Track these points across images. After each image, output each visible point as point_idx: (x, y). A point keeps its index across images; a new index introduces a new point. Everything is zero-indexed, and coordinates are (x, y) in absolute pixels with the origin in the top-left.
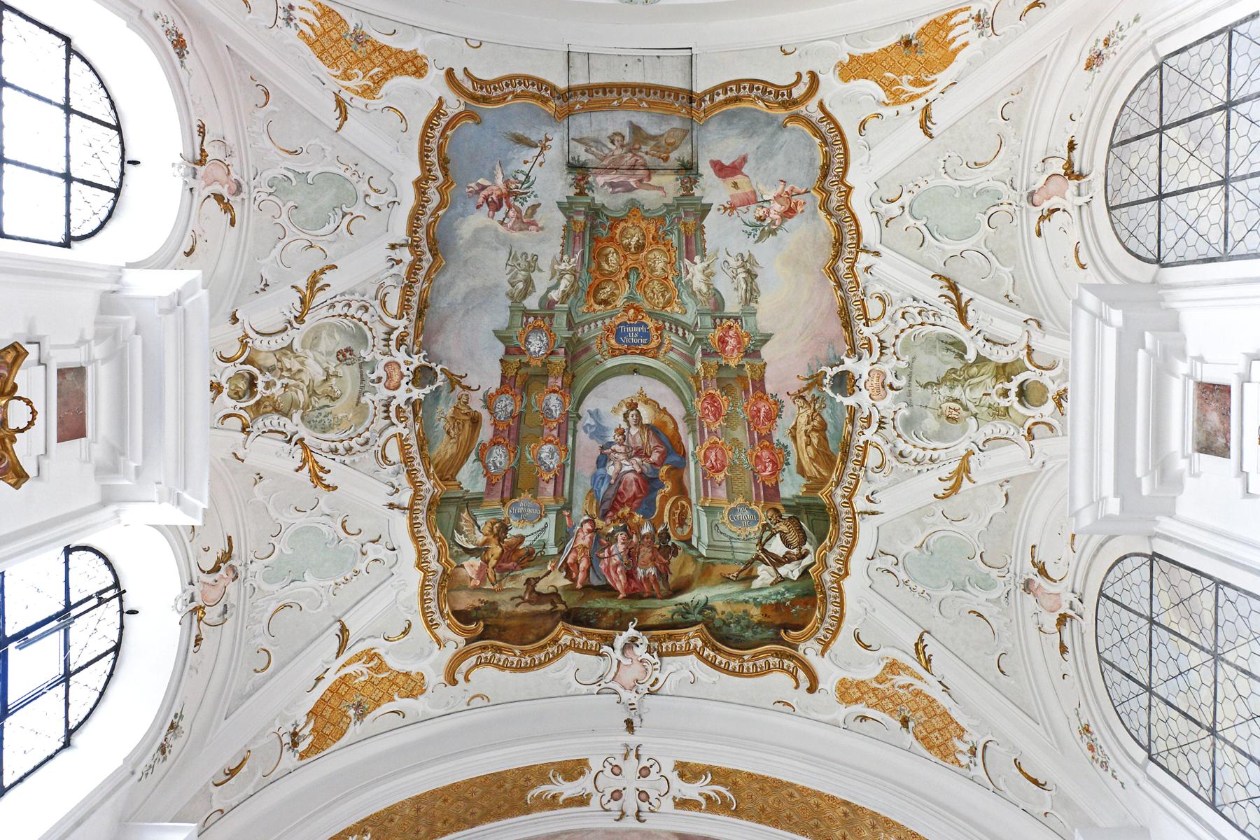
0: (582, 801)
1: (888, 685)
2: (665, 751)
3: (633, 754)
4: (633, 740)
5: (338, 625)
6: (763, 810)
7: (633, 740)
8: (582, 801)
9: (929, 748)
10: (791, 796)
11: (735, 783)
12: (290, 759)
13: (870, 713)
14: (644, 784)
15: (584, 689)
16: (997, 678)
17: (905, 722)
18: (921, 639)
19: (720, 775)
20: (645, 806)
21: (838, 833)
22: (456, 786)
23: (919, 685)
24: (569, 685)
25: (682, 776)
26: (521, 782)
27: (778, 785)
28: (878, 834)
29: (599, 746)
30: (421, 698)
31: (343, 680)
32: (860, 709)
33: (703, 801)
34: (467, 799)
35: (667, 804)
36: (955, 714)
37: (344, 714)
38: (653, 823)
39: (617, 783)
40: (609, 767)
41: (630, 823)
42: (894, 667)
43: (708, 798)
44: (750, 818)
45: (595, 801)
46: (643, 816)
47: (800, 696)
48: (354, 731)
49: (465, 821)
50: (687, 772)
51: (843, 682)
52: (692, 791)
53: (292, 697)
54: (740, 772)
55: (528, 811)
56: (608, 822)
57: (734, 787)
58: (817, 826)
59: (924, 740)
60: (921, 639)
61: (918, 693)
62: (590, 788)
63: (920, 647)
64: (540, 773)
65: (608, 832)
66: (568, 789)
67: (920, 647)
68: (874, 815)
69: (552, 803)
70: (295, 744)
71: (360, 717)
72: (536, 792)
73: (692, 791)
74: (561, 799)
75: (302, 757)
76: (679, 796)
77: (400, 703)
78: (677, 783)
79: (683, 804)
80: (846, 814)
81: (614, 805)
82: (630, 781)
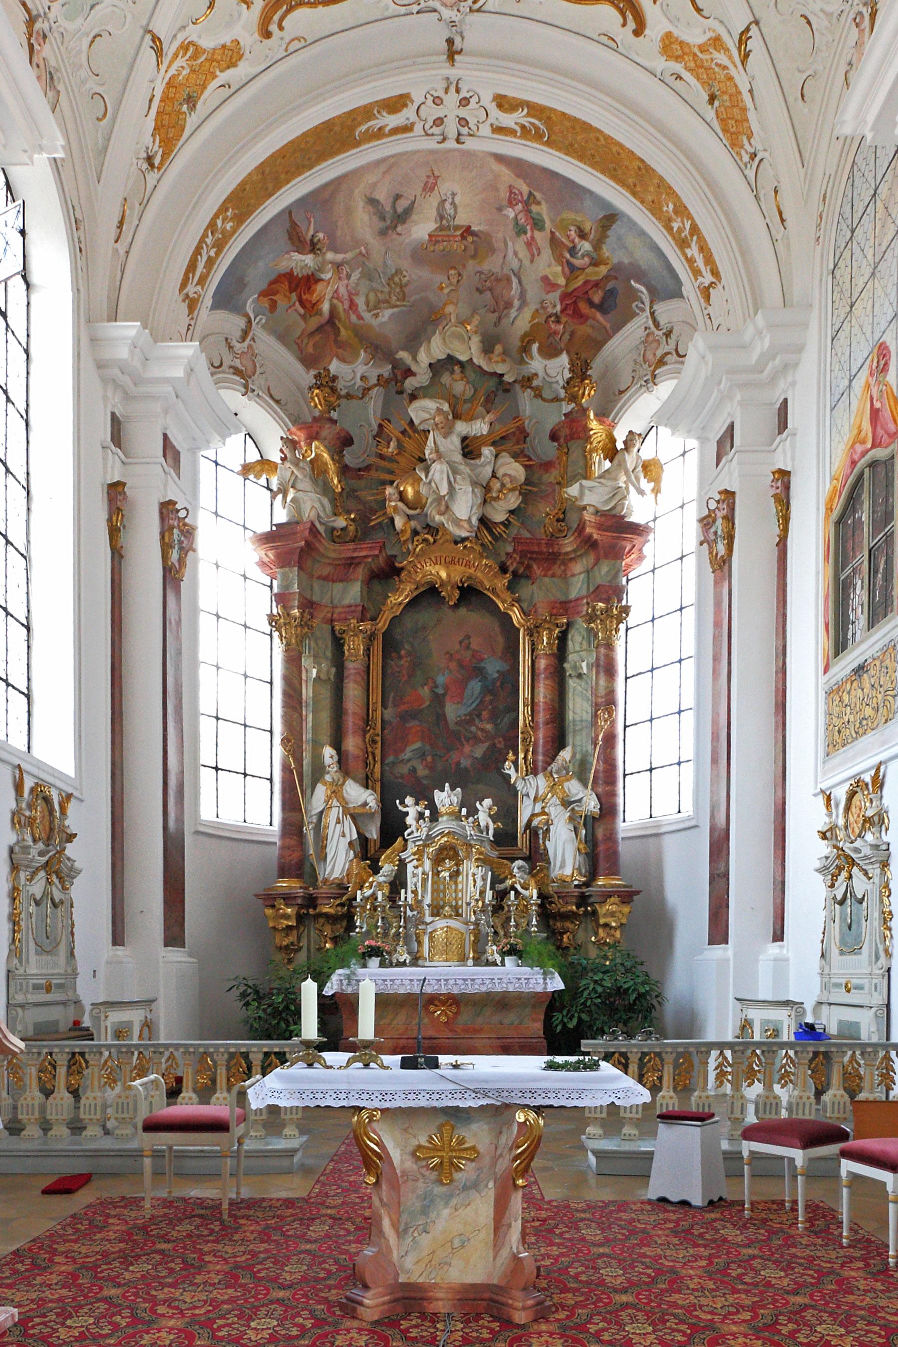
0: (407, 129)
1: (708, 57)
2: (483, 83)
3: (453, 89)
4: (453, 73)
5: (148, 37)
6: (571, 145)
7: (453, 73)
8: (407, 129)
9: (725, 131)
10: (598, 139)
11: (549, 118)
12: (152, 177)
13: (686, 75)
14: (463, 113)
15: (403, 10)
16: (796, 100)
17: (712, 99)
18: (747, 29)
19: (535, 110)
20: (465, 131)
21: (630, 181)
22: (292, 142)
23: (733, 72)
24: (386, 8)
25: (500, 106)
26: (349, 123)
27: (587, 128)
28: (661, 194)
29: (419, 84)
30: (241, 64)
31: (169, 85)
32: (678, 68)
33: (518, 129)
34: (302, 150)
35: (486, 130)
36: (751, 115)
37: (180, 112)
38: (470, 144)
39: (439, 112)
40: (430, 99)
41: (451, 144)
42: (717, 42)
43: (523, 127)
44: (559, 149)
45: (418, 129)
46: (462, 139)
47: (624, 35)
48: (192, 121)
49: (303, 167)
50: (504, 103)
51: (669, 35)
52: (509, 120)
53: (136, 129)
54: (555, 110)
55: (357, 144)
56: (431, 144)
57: (548, 121)
58: (615, 170)
59: (722, 121)
60: (747, 29)
61: (730, 79)
62: (413, 118)
63: (744, 38)
64: (366, 112)
65: (431, 152)
66: (392, 121)
67: (744, 38)
68: (661, 179)
69: (379, 134)
70: (152, 165)
71: (193, 108)
72: (363, 128)
73: (509, 120)
74: (387, 129)
75: (159, 169)
76: (497, 123)
77: (222, 77)
78: (495, 112)
79: (499, 130)
80: (639, 168)
81: (435, 130)
82: (450, 108)
